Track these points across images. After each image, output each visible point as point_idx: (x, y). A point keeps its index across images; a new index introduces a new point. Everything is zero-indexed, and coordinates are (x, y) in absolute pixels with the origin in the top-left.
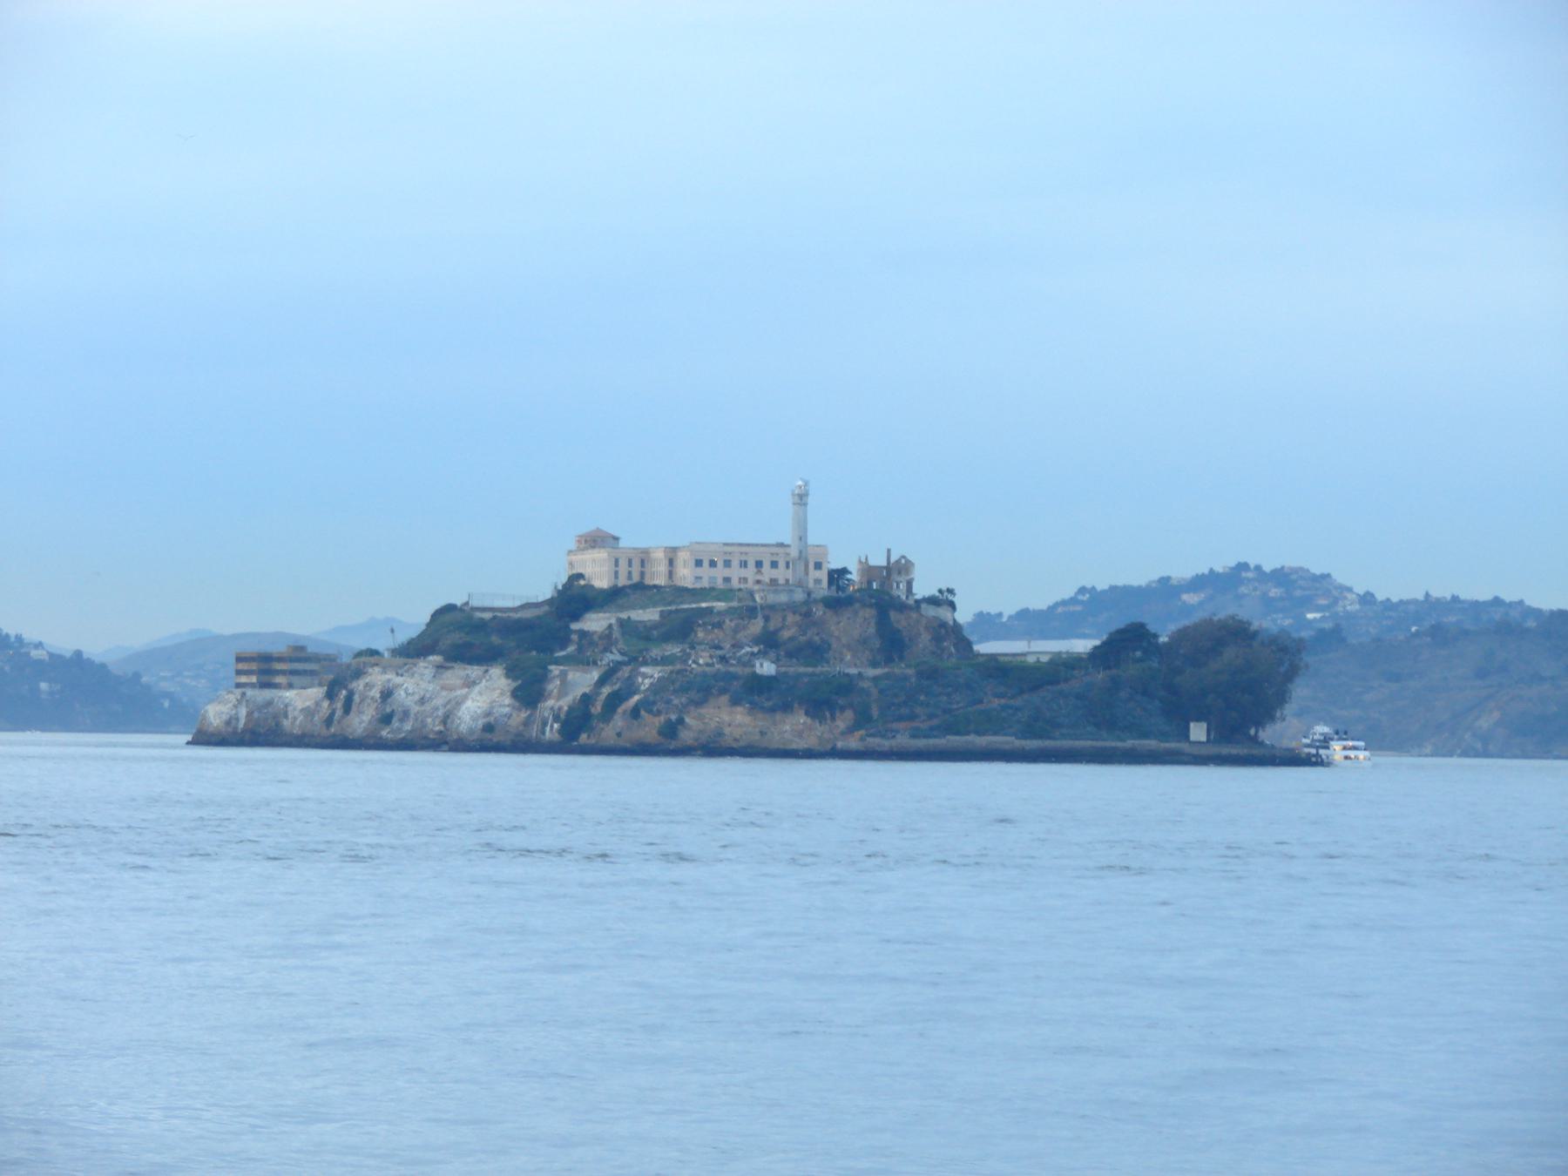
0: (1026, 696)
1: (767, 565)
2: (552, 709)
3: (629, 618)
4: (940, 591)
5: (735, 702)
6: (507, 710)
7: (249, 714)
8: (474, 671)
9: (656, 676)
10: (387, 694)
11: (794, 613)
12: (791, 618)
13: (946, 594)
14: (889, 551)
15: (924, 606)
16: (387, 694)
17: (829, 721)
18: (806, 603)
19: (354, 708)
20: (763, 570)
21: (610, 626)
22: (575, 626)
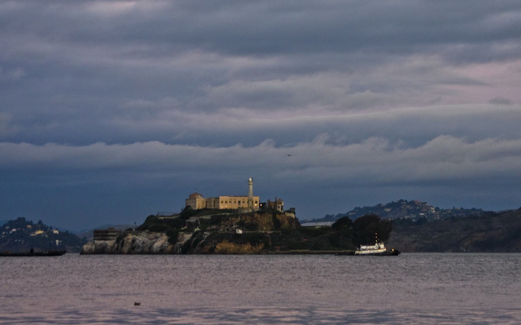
0: (313, 238)
1: (241, 202)
2: (180, 244)
3: (202, 218)
4: (291, 209)
5: (230, 242)
6: (166, 245)
7: (96, 248)
8: (158, 234)
9: (208, 234)
10: (134, 241)
11: (249, 216)
12: (248, 217)
13: (292, 210)
14: (276, 197)
15: (286, 213)
16: (134, 241)
17: (257, 246)
18: (252, 213)
19: (125, 245)
20: (241, 204)
21: (197, 221)
22: (187, 221)
